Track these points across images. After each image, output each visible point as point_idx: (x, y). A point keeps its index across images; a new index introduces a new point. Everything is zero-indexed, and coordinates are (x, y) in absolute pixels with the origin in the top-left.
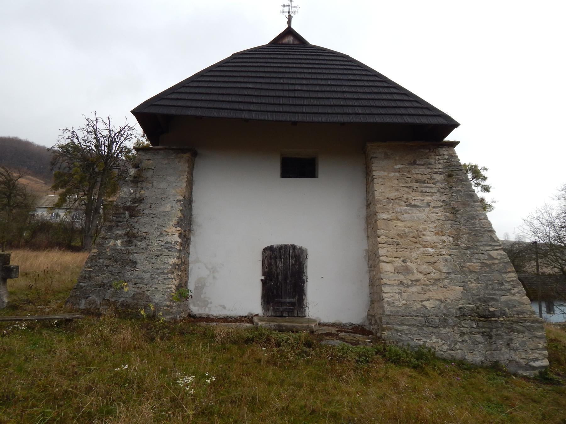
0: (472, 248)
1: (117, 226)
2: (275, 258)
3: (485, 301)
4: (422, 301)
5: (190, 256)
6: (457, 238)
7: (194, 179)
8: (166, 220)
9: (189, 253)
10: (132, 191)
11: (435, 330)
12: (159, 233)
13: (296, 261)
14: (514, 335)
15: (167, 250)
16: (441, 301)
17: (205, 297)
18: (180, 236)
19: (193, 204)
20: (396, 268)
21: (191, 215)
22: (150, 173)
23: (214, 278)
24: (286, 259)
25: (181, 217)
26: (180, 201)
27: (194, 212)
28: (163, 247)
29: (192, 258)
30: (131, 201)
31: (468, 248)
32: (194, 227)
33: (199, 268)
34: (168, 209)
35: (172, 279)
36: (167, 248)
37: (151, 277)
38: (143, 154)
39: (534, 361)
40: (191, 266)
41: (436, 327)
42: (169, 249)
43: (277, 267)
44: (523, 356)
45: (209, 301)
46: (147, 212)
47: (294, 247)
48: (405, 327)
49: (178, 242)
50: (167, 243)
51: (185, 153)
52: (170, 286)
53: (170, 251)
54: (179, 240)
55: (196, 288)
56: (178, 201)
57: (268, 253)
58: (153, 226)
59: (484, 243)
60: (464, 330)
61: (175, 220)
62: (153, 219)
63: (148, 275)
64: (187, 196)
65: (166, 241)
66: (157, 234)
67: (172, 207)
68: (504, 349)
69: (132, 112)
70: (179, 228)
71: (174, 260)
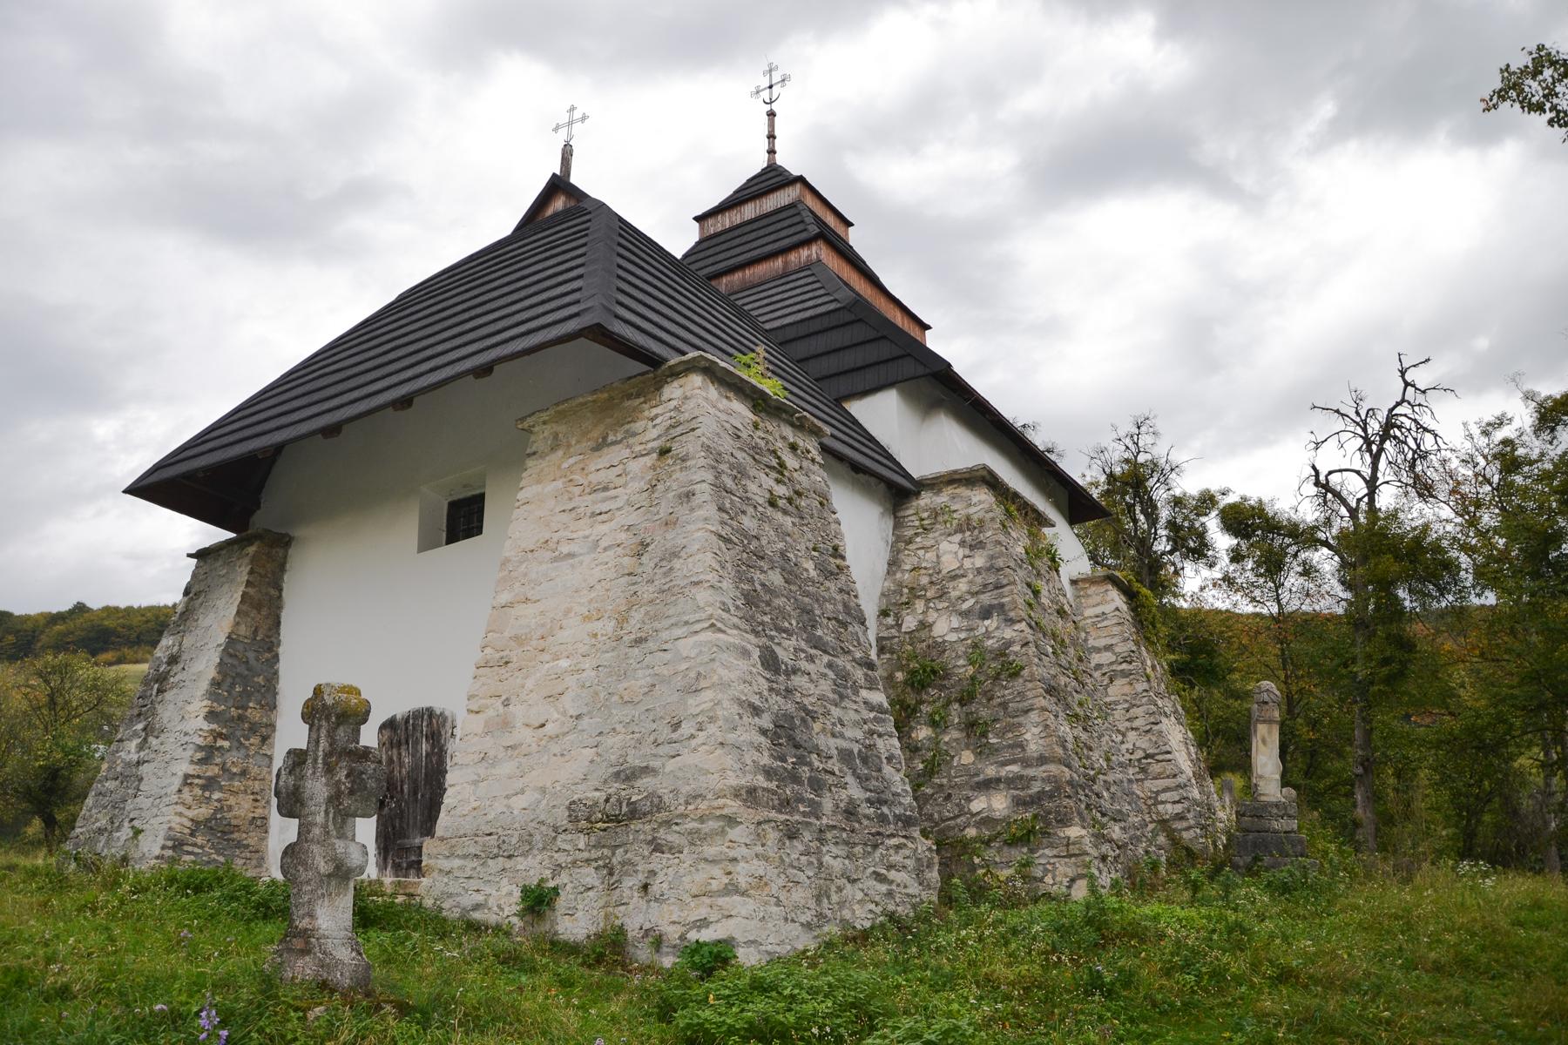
0: (646, 640)
2: (399, 744)
3: (628, 776)
4: (507, 797)
6: (622, 620)
11: (509, 864)
13: (433, 746)
14: (658, 861)
16: (543, 790)
18: (211, 716)
19: (281, 650)
20: (487, 724)
24: (417, 743)
31: (639, 641)
39: (699, 928)
41: (510, 857)
43: (401, 765)
44: (674, 918)
47: (430, 712)
48: (457, 863)
54: (206, 726)
57: (387, 733)
59: (673, 620)
60: (562, 858)
61: (204, 685)
68: (636, 899)
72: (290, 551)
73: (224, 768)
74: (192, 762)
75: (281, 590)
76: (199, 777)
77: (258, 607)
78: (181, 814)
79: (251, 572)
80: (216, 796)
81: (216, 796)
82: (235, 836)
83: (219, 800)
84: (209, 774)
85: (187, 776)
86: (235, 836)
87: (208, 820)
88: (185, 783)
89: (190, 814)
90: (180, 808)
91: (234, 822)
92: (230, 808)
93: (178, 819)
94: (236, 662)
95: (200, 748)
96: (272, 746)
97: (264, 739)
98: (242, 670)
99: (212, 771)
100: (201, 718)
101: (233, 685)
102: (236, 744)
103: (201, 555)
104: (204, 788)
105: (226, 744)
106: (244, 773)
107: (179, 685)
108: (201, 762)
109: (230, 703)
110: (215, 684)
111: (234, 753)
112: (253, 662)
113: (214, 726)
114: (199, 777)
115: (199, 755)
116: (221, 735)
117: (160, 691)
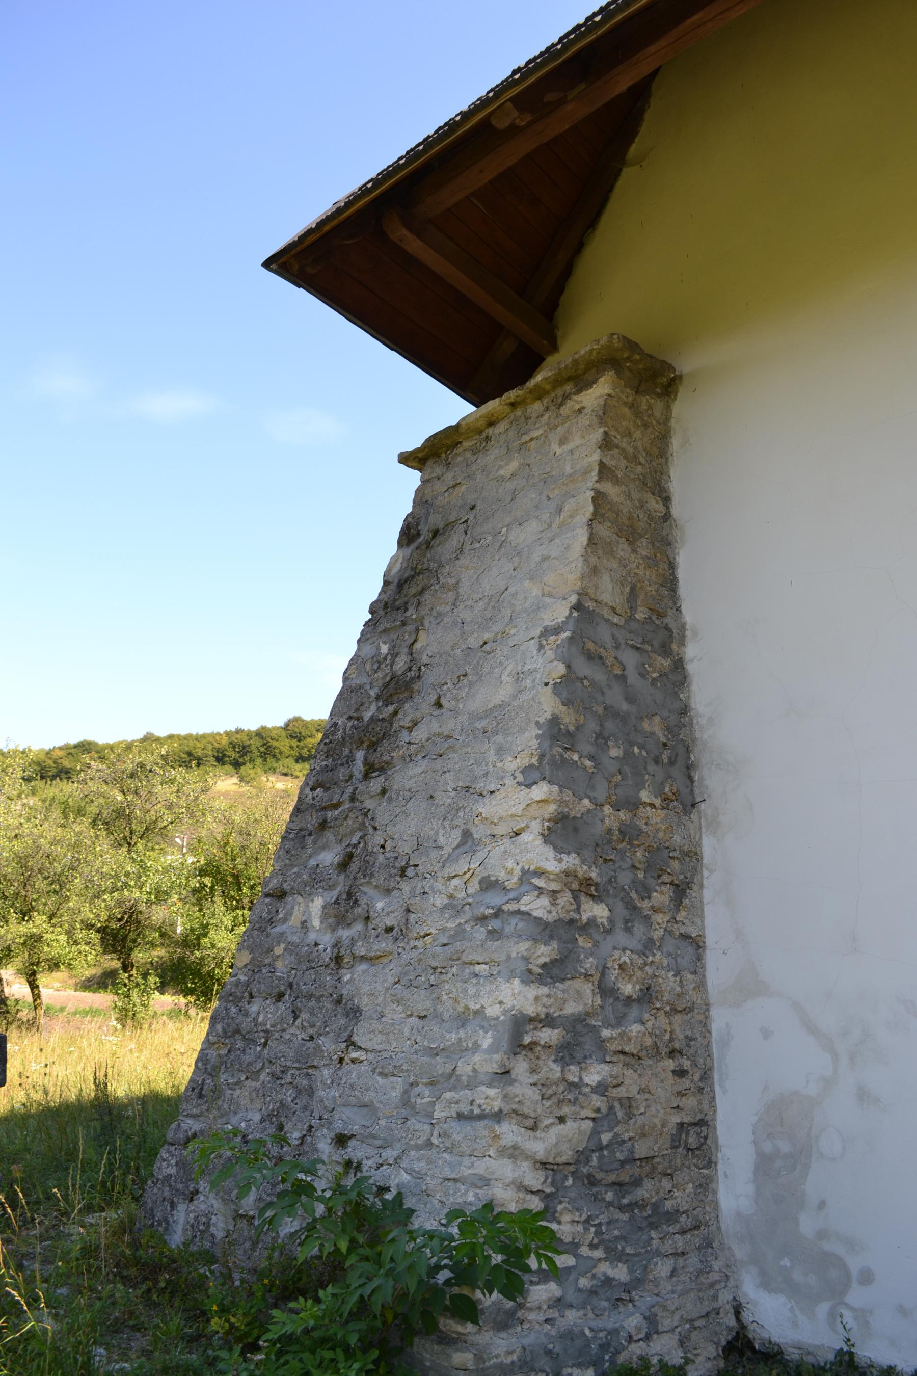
1: (323, 825)
5: (711, 958)
7: (675, 511)
8: (492, 756)
9: (697, 944)
10: (384, 649)
12: (456, 835)
15: (480, 933)
17: (822, 1235)
18: (562, 830)
19: (691, 651)
21: (685, 710)
22: (455, 539)
23: (863, 1095)
25: (554, 721)
26: (557, 630)
27: (702, 694)
28: (468, 913)
29: (718, 970)
30: (377, 698)
32: (711, 780)
33: (766, 1034)
34: (503, 693)
35: (498, 1116)
36: (482, 919)
37: (406, 1101)
38: (438, 471)
40: (719, 1019)
42: (494, 921)
45: (854, 1264)
46: (420, 734)
49: (540, 873)
50: (488, 885)
51: (589, 385)
52: (481, 1167)
53: (494, 934)
54: (550, 861)
55: (764, 1165)
56: (547, 632)
58: (438, 795)
61: (526, 743)
62: (438, 764)
63: (394, 1089)
64: (609, 592)
65: (482, 873)
66: (449, 839)
67: (518, 677)
69: (267, 264)
70: (540, 791)
71: (513, 996)
72: (677, 407)
73: (606, 991)
74: (529, 978)
75: (667, 500)
76: (548, 1021)
77: (631, 535)
78: (513, 1153)
79: (606, 444)
80: (594, 1075)
81: (594, 1075)
82: (645, 1192)
83: (601, 1089)
84: (571, 1008)
85: (520, 1023)
86: (645, 1192)
87: (582, 1156)
88: (518, 1047)
89: (539, 1146)
90: (509, 1132)
91: (641, 1149)
92: (628, 1103)
93: (506, 1170)
94: (599, 676)
95: (545, 930)
96: (698, 911)
97: (681, 891)
98: (615, 697)
99: (578, 997)
100: (532, 838)
101: (602, 739)
102: (621, 911)
103: (427, 456)
104: (567, 1053)
105: (599, 911)
106: (647, 995)
107: (439, 749)
108: (551, 973)
109: (601, 793)
110: (555, 732)
111: (620, 937)
112: (632, 676)
113: (571, 861)
114: (548, 1021)
115: (545, 953)
116: (585, 889)
117: (370, 770)
